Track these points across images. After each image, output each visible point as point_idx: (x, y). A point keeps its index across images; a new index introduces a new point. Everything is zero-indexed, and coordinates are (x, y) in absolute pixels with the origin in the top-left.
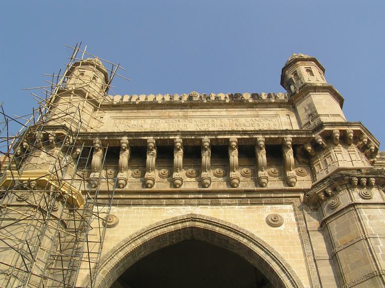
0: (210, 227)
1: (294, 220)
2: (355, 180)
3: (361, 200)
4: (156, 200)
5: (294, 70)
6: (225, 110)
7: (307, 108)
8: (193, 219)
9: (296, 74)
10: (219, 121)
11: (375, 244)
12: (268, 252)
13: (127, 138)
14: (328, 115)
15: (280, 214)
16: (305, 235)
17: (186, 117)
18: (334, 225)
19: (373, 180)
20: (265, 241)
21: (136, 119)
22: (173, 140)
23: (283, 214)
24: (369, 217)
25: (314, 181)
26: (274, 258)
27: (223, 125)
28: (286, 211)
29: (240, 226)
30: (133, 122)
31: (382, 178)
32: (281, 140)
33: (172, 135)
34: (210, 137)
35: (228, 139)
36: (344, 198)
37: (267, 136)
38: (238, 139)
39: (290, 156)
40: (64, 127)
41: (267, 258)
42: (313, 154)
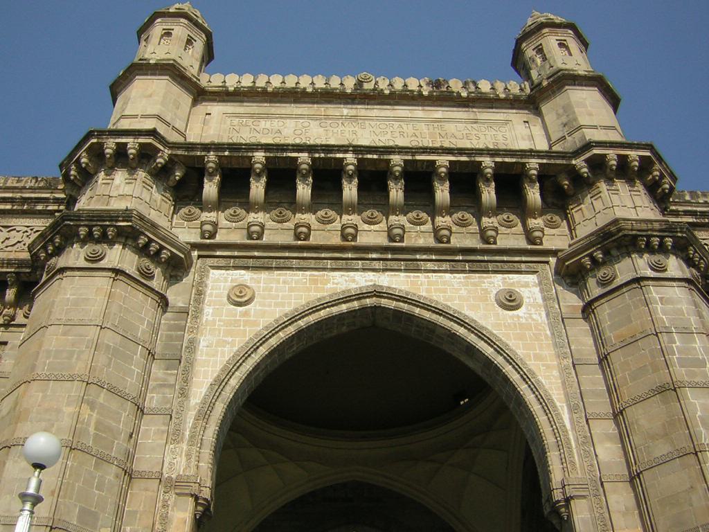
0: (405, 307)
1: (540, 301)
3: (650, 273)
4: (313, 261)
5: (539, 43)
6: (420, 108)
7: (561, 111)
8: (377, 293)
9: (540, 50)
10: (410, 126)
11: (668, 343)
12: (499, 351)
13: (263, 154)
14: (595, 127)
15: (517, 290)
16: (559, 320)
17: (354, 118)
18: (606, 310)
19: (669, 242)
20: (495, 332)
22: (342, 160)
23: (522, 289)
25: (572, 238)
26: (510, 360)
28: (526, 285)
30: (264, 124)
31: (682, 237)
32: (521, 166)
33: (339, 151)
35: (434, 162)
36: (624, 269)
38: (451, 162)
39: (534, 195)
40: (153, 133)
41: (499, 360)
42: (571, 193)
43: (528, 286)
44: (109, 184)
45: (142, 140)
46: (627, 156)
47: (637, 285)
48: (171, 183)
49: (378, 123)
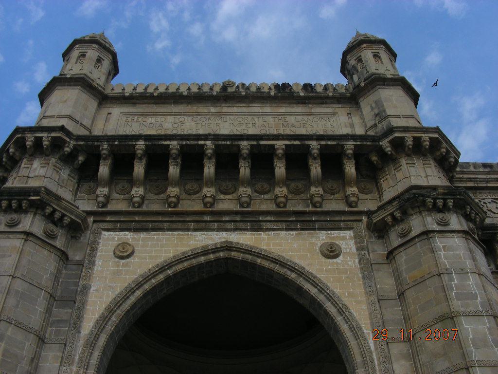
0: (249, 257)
1: (354, 249)
2: (430, 201)
3: (436, 227)
4: (180, 224)
5: (359, 55)
7: (374, 105)
8: (228, 247)
9: (360, 60)
10: (261, 119)
11: (449, 281)
12: (321, 290)
13: (143, 143)
14: (398, 116)
15: (337, 243)
16: (367, 268)
17: (219, 114)
18: (403, 258)
19: (450, 203)
20: (318, 276)
21: (154, 115)
22: (203, 145)
23: (341, 242)
24: (444, 247)
25: (380, 201)
26: (329, 298)
27: (267, 125)
28: (344, 238)
29: (287, 257)
30: (151, 120)
31: (460, 199)
33: (202, 140)
34: (250, 143)
35: (273, 146)
36: (417, 223)
37: (323, 143)
38: (286, 145)
39: (350, 169)
40: (62, 128)
41: (321, 298)
42: (380, 166)
43: (345, 239)
44: (28, 168)
45: (53, 135)
46: (420, 138)
47: (425, 237)
48: (76, 166)
49: (237, 117)
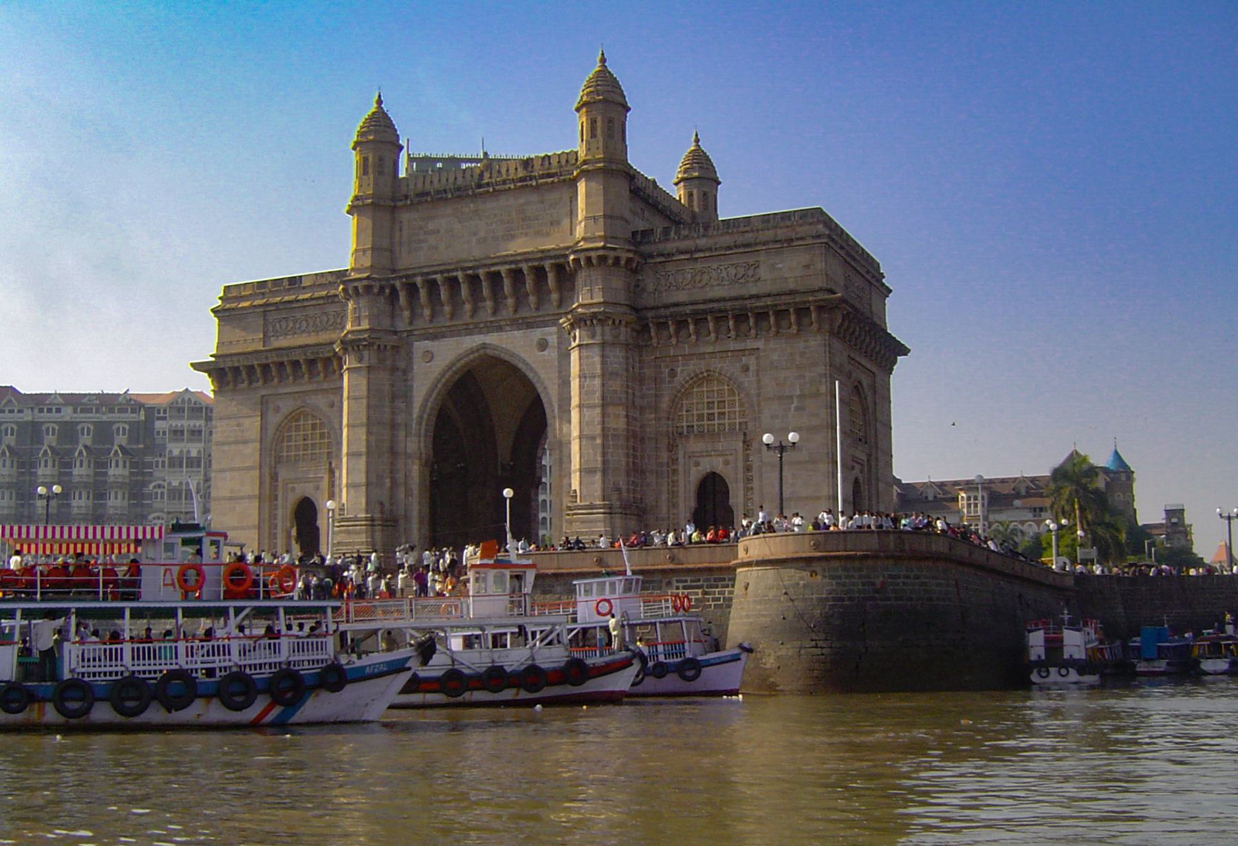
28: (551, 334)
